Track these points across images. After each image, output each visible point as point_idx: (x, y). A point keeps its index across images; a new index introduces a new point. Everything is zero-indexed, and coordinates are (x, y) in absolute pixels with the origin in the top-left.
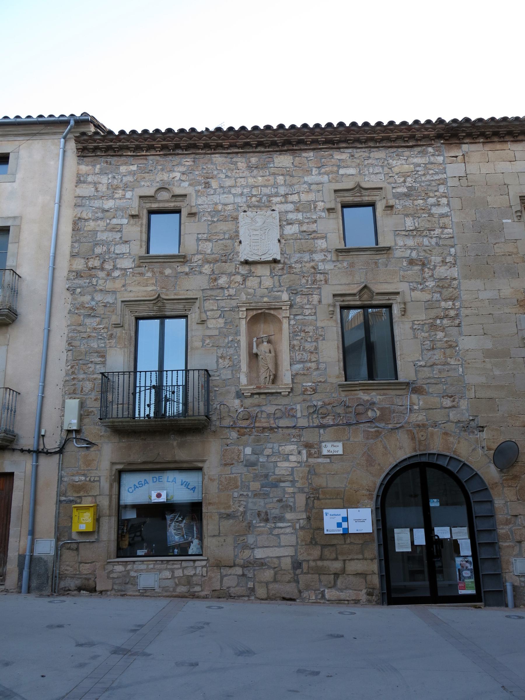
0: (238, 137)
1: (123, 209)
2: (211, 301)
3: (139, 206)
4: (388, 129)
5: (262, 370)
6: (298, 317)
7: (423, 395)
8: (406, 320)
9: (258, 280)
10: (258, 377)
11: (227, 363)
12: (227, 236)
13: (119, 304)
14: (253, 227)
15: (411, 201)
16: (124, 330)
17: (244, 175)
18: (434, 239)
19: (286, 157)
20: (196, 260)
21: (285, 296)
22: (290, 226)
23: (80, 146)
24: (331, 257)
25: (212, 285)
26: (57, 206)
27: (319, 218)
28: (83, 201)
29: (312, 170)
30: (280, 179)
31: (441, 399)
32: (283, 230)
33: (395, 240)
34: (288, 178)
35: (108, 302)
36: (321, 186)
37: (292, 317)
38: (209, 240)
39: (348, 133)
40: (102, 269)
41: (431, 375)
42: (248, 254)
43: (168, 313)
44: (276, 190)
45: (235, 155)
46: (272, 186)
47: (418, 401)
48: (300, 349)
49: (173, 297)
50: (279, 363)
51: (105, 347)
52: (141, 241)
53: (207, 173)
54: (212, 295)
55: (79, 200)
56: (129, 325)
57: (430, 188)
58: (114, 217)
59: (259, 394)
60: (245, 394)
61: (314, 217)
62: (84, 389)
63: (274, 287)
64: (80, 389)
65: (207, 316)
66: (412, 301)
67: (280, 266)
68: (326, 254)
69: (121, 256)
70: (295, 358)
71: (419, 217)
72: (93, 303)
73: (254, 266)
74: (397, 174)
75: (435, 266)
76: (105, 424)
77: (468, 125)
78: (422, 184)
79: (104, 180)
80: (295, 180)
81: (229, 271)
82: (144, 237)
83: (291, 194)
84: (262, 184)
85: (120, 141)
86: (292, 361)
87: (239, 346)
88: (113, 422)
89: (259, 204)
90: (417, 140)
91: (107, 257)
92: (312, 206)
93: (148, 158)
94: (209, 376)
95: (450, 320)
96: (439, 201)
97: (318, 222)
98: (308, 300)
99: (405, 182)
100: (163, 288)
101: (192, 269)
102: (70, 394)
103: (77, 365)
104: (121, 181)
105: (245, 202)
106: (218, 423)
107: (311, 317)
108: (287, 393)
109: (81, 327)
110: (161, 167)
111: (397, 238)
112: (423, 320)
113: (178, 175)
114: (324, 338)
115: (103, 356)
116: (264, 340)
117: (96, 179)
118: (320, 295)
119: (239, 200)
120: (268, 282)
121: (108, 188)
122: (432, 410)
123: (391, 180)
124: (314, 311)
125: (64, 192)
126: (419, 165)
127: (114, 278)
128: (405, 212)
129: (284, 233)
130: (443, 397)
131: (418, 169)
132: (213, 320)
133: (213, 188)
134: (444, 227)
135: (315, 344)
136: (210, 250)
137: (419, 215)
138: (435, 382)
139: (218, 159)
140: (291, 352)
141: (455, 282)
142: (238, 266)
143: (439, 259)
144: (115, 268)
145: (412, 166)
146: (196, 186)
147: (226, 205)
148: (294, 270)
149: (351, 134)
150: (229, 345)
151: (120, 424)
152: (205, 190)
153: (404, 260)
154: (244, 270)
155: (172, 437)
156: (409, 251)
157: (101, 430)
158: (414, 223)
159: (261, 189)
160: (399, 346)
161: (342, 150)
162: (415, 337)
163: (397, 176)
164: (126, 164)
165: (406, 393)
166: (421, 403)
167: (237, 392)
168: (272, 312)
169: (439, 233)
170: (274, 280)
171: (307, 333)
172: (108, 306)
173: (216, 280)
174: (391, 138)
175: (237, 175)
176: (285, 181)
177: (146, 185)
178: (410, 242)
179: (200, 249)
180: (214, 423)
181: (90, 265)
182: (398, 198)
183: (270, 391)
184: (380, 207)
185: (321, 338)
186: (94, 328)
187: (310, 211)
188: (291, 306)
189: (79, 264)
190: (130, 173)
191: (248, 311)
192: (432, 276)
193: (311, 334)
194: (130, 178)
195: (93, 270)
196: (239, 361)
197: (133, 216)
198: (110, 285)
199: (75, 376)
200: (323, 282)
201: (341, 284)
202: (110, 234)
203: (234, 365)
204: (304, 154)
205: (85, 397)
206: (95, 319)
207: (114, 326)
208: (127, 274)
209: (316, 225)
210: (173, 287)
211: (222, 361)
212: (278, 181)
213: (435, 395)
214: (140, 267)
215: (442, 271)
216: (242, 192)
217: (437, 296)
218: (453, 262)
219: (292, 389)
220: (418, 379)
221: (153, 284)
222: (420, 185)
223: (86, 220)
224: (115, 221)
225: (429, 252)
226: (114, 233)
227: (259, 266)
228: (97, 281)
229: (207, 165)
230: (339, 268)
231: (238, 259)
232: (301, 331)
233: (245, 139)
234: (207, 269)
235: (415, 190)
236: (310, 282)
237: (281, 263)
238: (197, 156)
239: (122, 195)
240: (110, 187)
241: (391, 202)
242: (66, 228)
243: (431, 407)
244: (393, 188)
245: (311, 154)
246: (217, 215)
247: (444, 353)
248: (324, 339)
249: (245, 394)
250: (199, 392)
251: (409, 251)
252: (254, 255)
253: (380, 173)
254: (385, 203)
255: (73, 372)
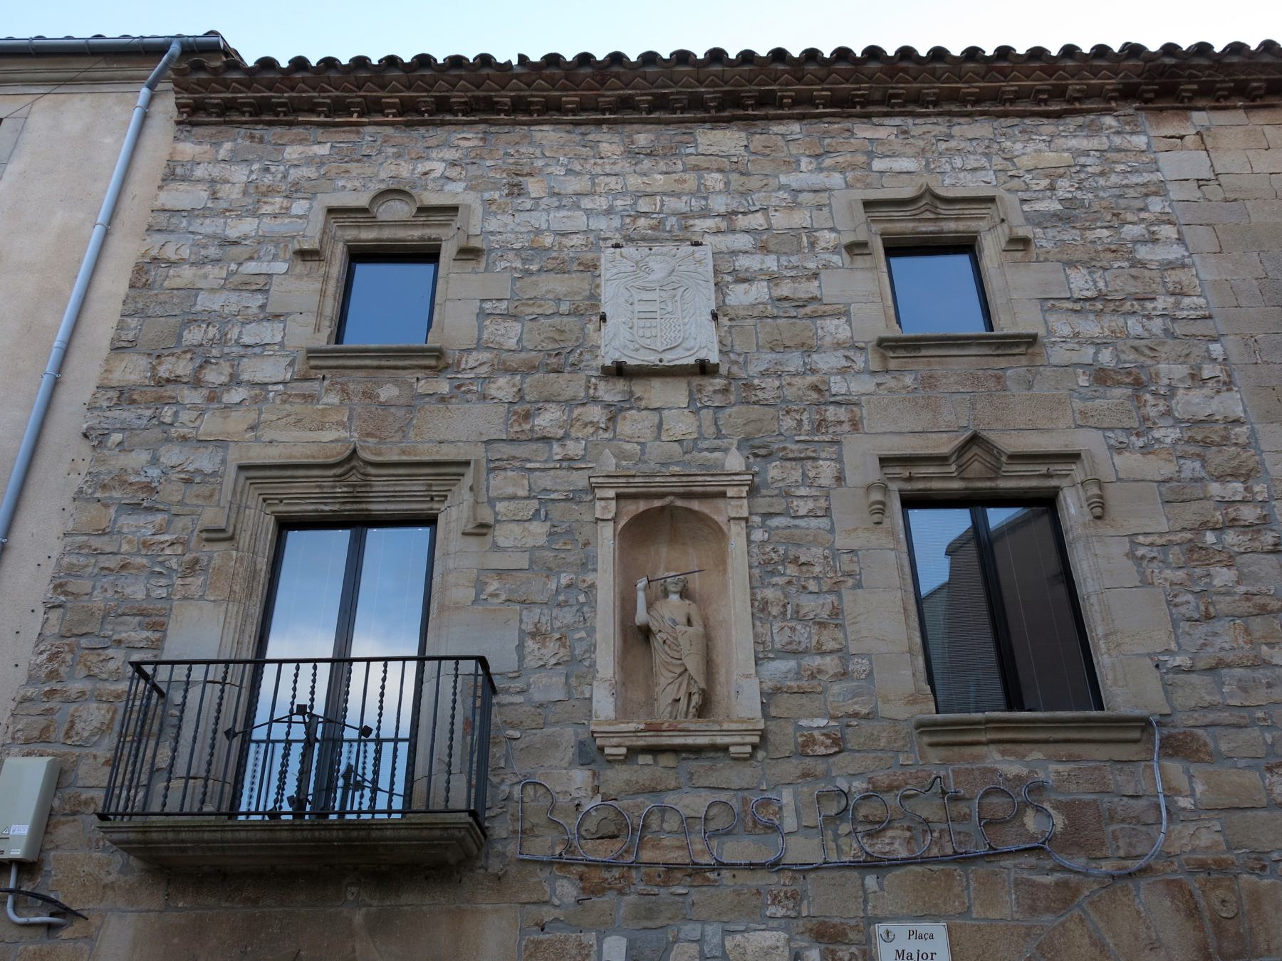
0: (603, 84)
1: (277, 240)
2: (510, 473)
3: (324, 232)
4: (994, 69)
5: (664, 677)
6: (775, 522)
7: (1201, 761)
8: (1111, 532)
9: (654, 418)
10: (651, 701)
11: (550, 652)
12: (564, 308)
13: (232, 471)
14: (639, 283)
15: (1078, 232)
16: (237, 550)
17: (617, 169)
18: (1159, 321)
19: (728, 133)
20: (471, 364)
21: (734, 461)
22: (746, 285)
23: (186, 98)
24: (866, 362)
25: (517, 428)
26: (97, 232)
27: (825, 267)
28: (173, 220)
29: (798, 162)
30: (714, 180)
31: (1263, 778)
32: (724, 295)
33: (1046, 322)
34: (734, 177)
35: (198, 471)
36: (826, 195)
37: (757, 519)
38: (515, 317)
39: (891, 78)
40: (196, 383)
41: (1218, 699)
42: (625, 347)
43: (377, 508)
44: (703, 202)
45: (593, 128)
46: (692, 194)
47: (1192, 784)
48: (784, 614)
49: (395, 458)
50: (719, 659)
51: (168, 598)
52: (320, 314)
53: (516, 164)
54: (514, 458)
55: (162, 219)
56: (255, 537)
57: (1123, 203)
58: (251, 258)
59: (655, 751)
60: (607, 751)
61: (812, 265)
62: (79, 726)
63: (701, 437)
64: (66, 726)
65: (496, 514)
66: (1119, 480)
67: (718, 383)
68: (851, 354)
69: (257, 350)
70: (768, 638)
71: (1105, 269)
72: (154, 472)
73: (642, 382)
74: (1028, 171)
75: (1172, 389)
76: (115, 836)
77: (1204, 62)
78: (1101, 194)
79: (239, 174)
80: (754, 182)
81: (568, 394)
82: (331, 307)
83: (744, 213)
84: (667, 189)
85: (293, 89)
86: (761, 648)
87: (592, 604)
88: (145, 829)
89: (657, 234)
90: (1072, 100)
91: (215, 352)
92: (805, 239)
93: (361, 129)
94: (490, 687)
95: (1244, 533)
96: (1154, 233)
97: (822, 276)
98: (804, 475)
99: (1052, 188)
100: (368, 435)
101: (459, 387)
102: (27, 742)
103: (71, 651)
104: (285, 177)
105: (617, 230)
106: (512, 848)
107: (814, 523)
108: (749, 749)
109: (106, 538)
110: (395, 150)
111: (1052, 318)
112: (1161, 534)
113: (439, 168)
114: (860, 581)
115: (159, 627)
116: (671, 588)
117: (216, 171)
118: (839, 460)
119: (601, 224)
120: (681, 425)
121: (245, 193)
122: (1239, 814)
123: (1015, 183)
124: (822, 503)
125: (127, 202)
126: (1086, 153)
127: (228, 407)
128: (1065, 257)
129: (727, 302)
130: (1270, 769)
131: (1082, 160)
132: (513, 526)
133: (533, 195)
134: (1179, 293)
135: (831, 598)
136: (515, 340)
137: (1105, 264)
138: (1233, 720)
139: (548, 135)
140: (758, 623)
141: (1242, 431)
142: (593, 380)
143: (1181, 371)
144: (235, 380)
145: (1066, 155)
146: (486, 190)
147: (564, 234)
148: (758, 392)
149: (898, 82)
150: (561, 598)
151: (170, 835)
152: (508, 200)
153: (1080, 371)
154: (611, 392)
155: (351, 893)
156: (1091, 350)
157: (108, 865)
158: (1095, 282)
159: (662, 201)
160: (1096, 607)
161: (875, 120)
162: (1146, 583)
163: (1028, 177)
164: (302, 141)
165: (1144, 756)
166: (1199, 788)
167: (582, 744)
168: (695, 505)
169: (1170, 306)
170: (699, 420)
171: (804, 568)
172: (198, 479)
173: (527, 416)
174: (1004, 92)
175: (598, 170)
176: (727, 184)
177: (349, 185)
178: (1090, 327)
179: (485, 336)
180: (499, 847)
181: (163, 371)
182: (1039, 225)
183: (690, 741)
184: (991, 248)
185: (850, 582)
186: (144, 543)
187: (799, 251)
188: (753, 490)
189: (132, 370)
190: (310, 160)
191: (623, 503)
192: (1168, 413)
193: (817, 569)
194: (310, 172)
195: (170, 387)
196: (592, 648)
197: (303, 255)
198: (211, 425)
199: (58, 687)
200: (846, 427)
201: (900, 433)
202: (234, 297)
203: (573, 661)
204: (776, 128)
205: (77, 751)
206: (150, 518)
207: (204, 535)
208: (266, 398)
209: (816, 283)
210: (400, 434)
211: (535, 646)
212: (708, 183)
213: (1242, 763)
214: (306, 380)
215: (1192, 402)
216: (611, 207)
217: (1192, 467)
218: (1223, 377)
219: (763, 735)
220: (1174, 709)
221: (338, 423)
222: (1096, 196)
223: (171, 263)
224: (251, 267)
225: (1147, 352)
226: (245, 294)
227: (656, 383)
228: (176, 414)
229: (517, 147)
230: (891, 391)
231: (594, 364)
232: (785, 560)
233: (621, 89)
234: (503, 387)
235: (1083, 206)
236: (806, 427)
237: (721, 376)
238: (493, 129)
239: (281, 208)
240: (252, 190)
241: (1021, 232)
242: (114, 284)
243: (1236, 802)
244: (1024, 201)
245: (795, 127)
246: (539, 257)
247: (1247, 631)
248: (859, 585)
249: (607, 751)
250: (452, 732)
251: (1091, 350)
252: (642, 351)
253: (984, 168)
254: (1007, 231)
255: (51, 672)
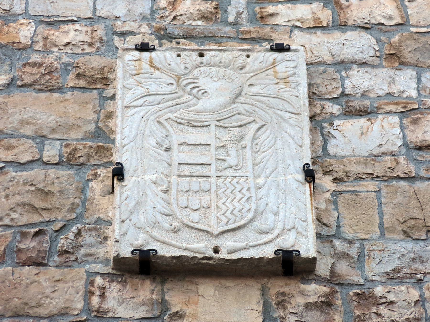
12: (51, 152)
22: (363, 121)
32: (326, 137)
42: (155, 224)
67: (314, 290)
73: (184, 285)
105: (144, 18)
129: (331, 149)
142: (99, 280)
147: (54, 23)
227: (207, 289)
231: (101, 251)
237: (318, 280)
252: (185, 232)
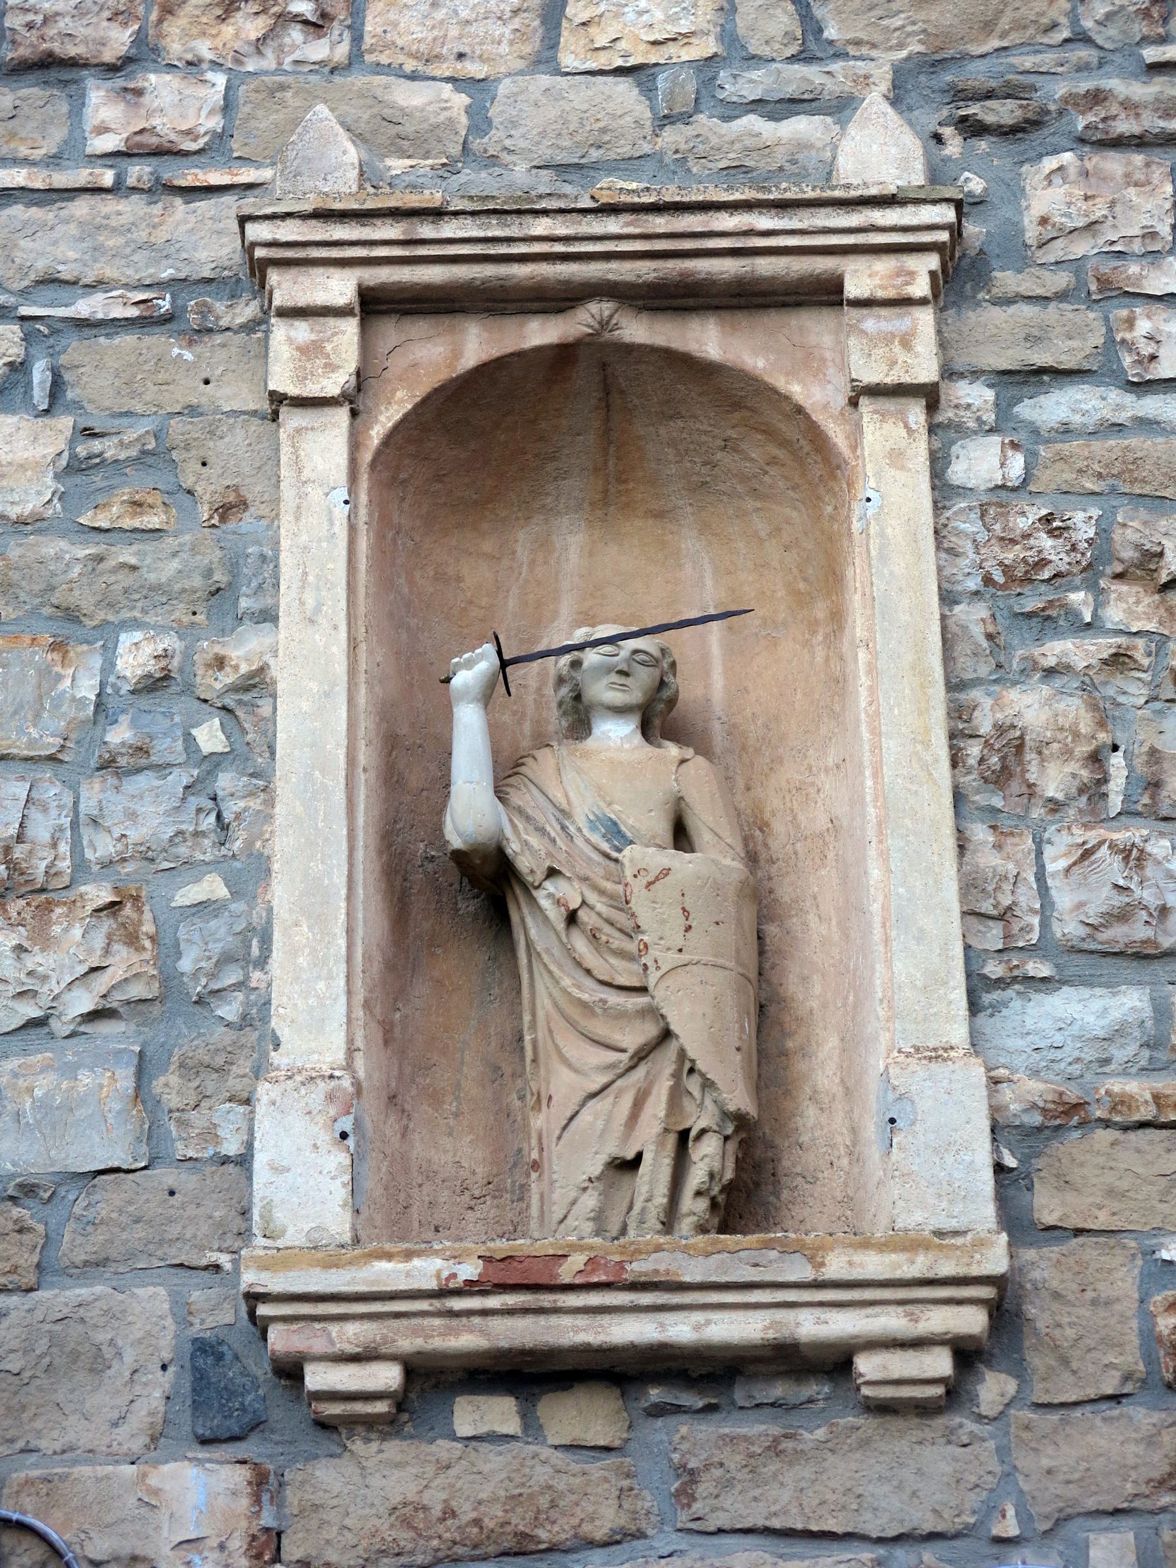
5: (571, 1068)
6: (1053, 407)
10: (513, 1173)
21: (879, 149)
37: (976, 396)
50: (810, 989)
59: (529, 1376)
60: (317, 1378)
63: (735, 52)
70: (1027, 897)
86: (993, 936)
87: (253, 757)
108: (940, 1363)
116: (603, 691)
140: (980, 833)
150: (119, 735)
168: (707, 339)
183: (681, 1330)
188: (960, 275)
191: (390, 331)
196: (253, 947)
219: (1005, 1303)
232: (1094, 568)
249: (317, 1378)
